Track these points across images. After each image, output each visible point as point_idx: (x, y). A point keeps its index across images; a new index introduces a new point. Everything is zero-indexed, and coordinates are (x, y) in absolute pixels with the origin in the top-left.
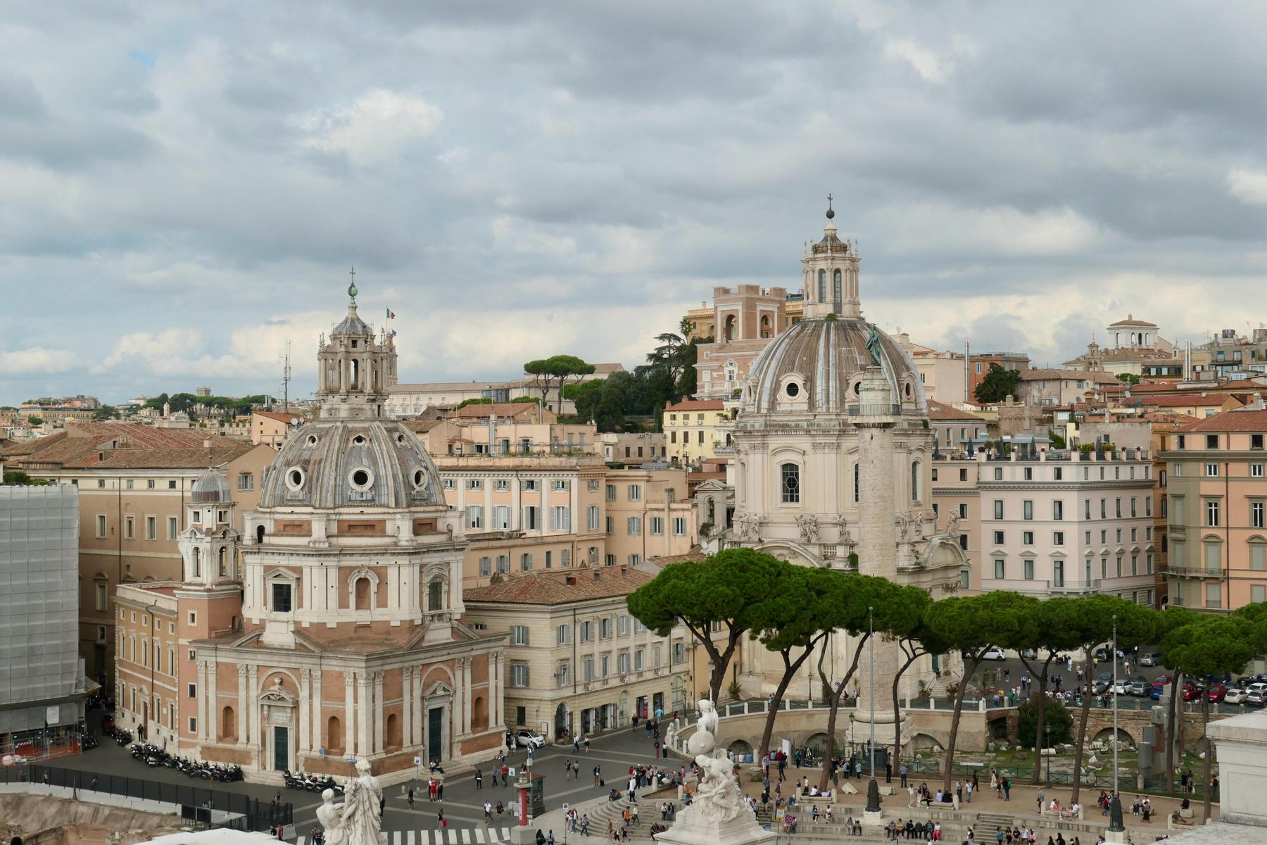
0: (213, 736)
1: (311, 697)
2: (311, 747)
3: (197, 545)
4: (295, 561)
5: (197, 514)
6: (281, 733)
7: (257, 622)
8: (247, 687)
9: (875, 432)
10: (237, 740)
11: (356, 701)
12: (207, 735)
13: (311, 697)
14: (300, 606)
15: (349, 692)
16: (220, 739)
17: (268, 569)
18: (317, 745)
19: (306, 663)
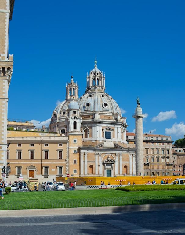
0: (86, 173)
1: (119, 160)
2: (119, 174)
3: (75, 120)
4: (112, 126)
5: (75, 113)
6: (109, 171)
7: (101, 141)
8: (99, 159)
9: (141, 118)
10: (95, 174)
11: (133, 161)
12: (84, 173)
13: (119, 160)
14: (114, 137)
15: (131, 158)
16: (88, 174)
17: (103, 127)
18: (121, 173)
19: (117, 152)
